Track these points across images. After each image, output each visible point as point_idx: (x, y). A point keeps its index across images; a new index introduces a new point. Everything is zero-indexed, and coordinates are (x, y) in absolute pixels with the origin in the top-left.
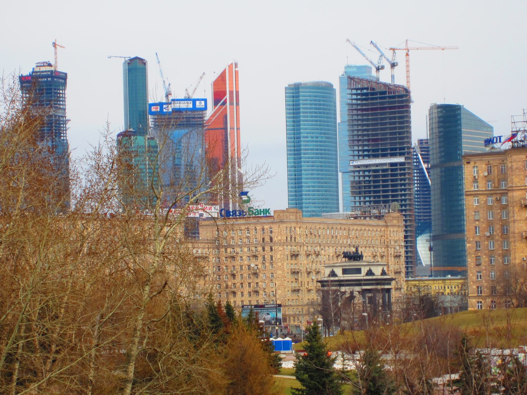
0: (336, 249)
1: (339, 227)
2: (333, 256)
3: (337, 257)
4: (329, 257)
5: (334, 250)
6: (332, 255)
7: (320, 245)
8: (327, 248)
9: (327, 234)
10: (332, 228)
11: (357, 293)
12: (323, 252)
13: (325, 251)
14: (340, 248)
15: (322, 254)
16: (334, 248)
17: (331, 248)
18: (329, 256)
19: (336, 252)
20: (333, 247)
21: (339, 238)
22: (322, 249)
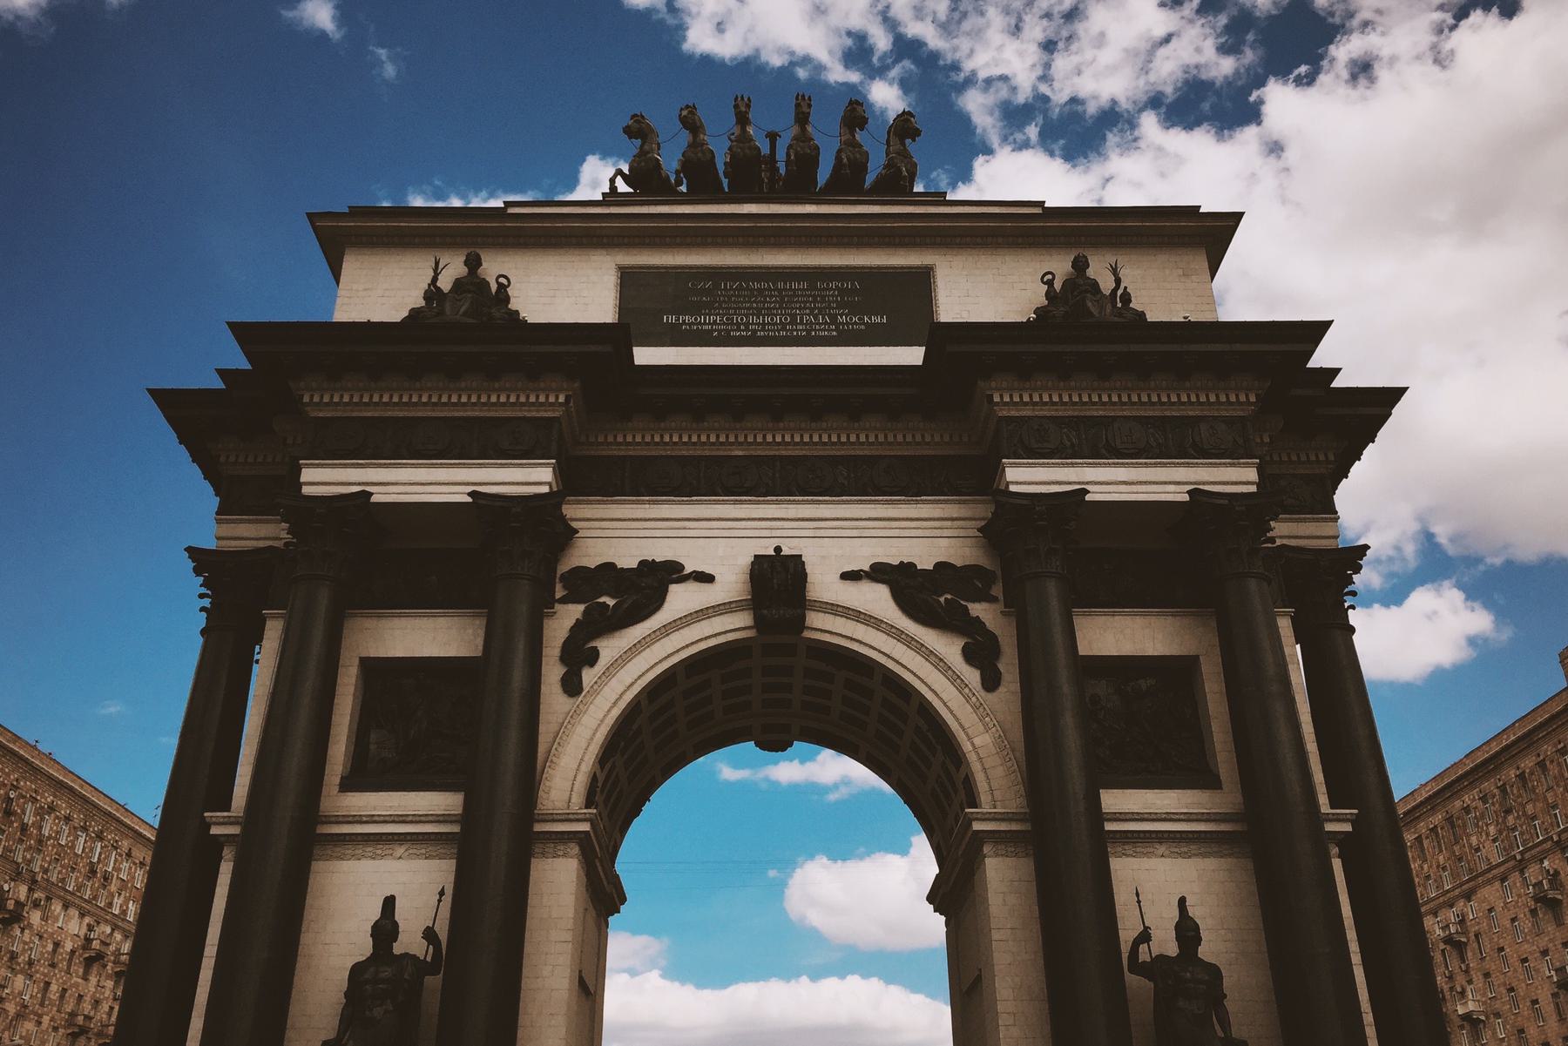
0: (90, 928)
1: (125, 844)
2: (73, 952)
3: (89, 963)
4: (54, 951)
5: (84, 930)
6: (68, 946)
7: (34, 882)
8: (57, 907)
9: (73, 847)
10: (100, 837)
11: (877, 599)
12: (35, 917)
13: (44, 918)
14: (108, 930)
15: (30, 926)
16: (87, 920)
17: (74, 912)
18: (57, 945)
19: (88, 940)
20: (82, 915)
21: (113, 888)
22: (36, 904)
